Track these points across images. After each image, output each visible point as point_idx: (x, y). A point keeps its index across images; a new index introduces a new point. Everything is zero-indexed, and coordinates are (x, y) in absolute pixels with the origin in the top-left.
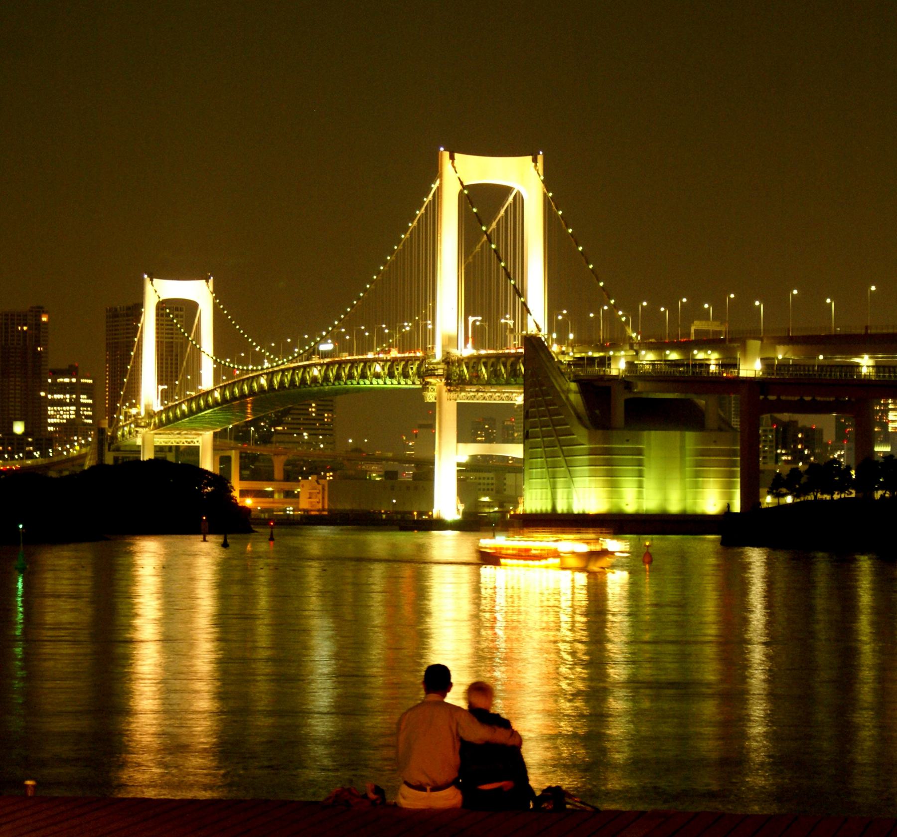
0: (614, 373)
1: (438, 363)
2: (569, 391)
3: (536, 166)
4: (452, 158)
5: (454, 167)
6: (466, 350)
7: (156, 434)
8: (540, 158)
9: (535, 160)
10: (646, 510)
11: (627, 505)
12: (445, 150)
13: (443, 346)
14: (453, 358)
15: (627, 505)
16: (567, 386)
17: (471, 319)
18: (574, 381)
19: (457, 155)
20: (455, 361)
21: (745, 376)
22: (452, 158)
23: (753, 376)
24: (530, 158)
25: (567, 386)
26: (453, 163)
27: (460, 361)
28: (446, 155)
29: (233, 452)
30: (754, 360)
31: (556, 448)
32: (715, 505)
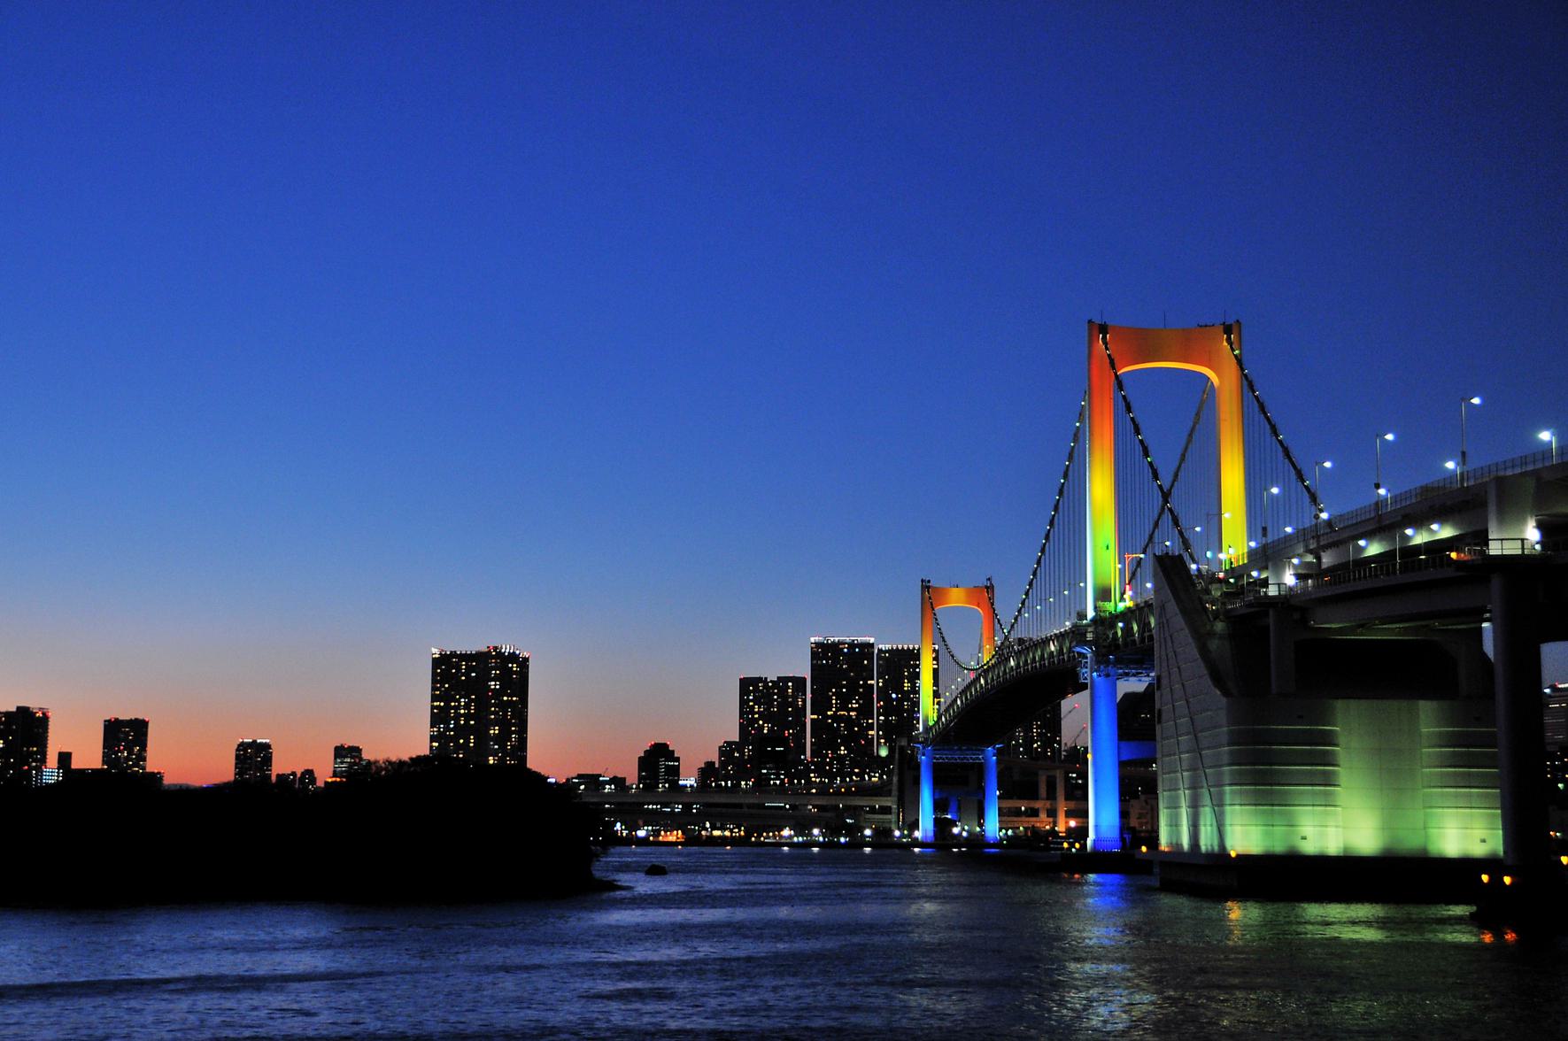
0: (1272, 591)
1: (1088, 625)
2: (1211, 634)
7: (935, 750)
10: (1345, 849)
11: (1304, 838)
14: (1102, 614)
15: (1304, 838)
16: (1208, 627)
17: (1129, 557)
20: (1105, 618)
21: (1499, 553)
23: (1520, 552)
25: (1208, 627)
29: (1058, 771)
30: (1523, 522)
32: (1483, 841)
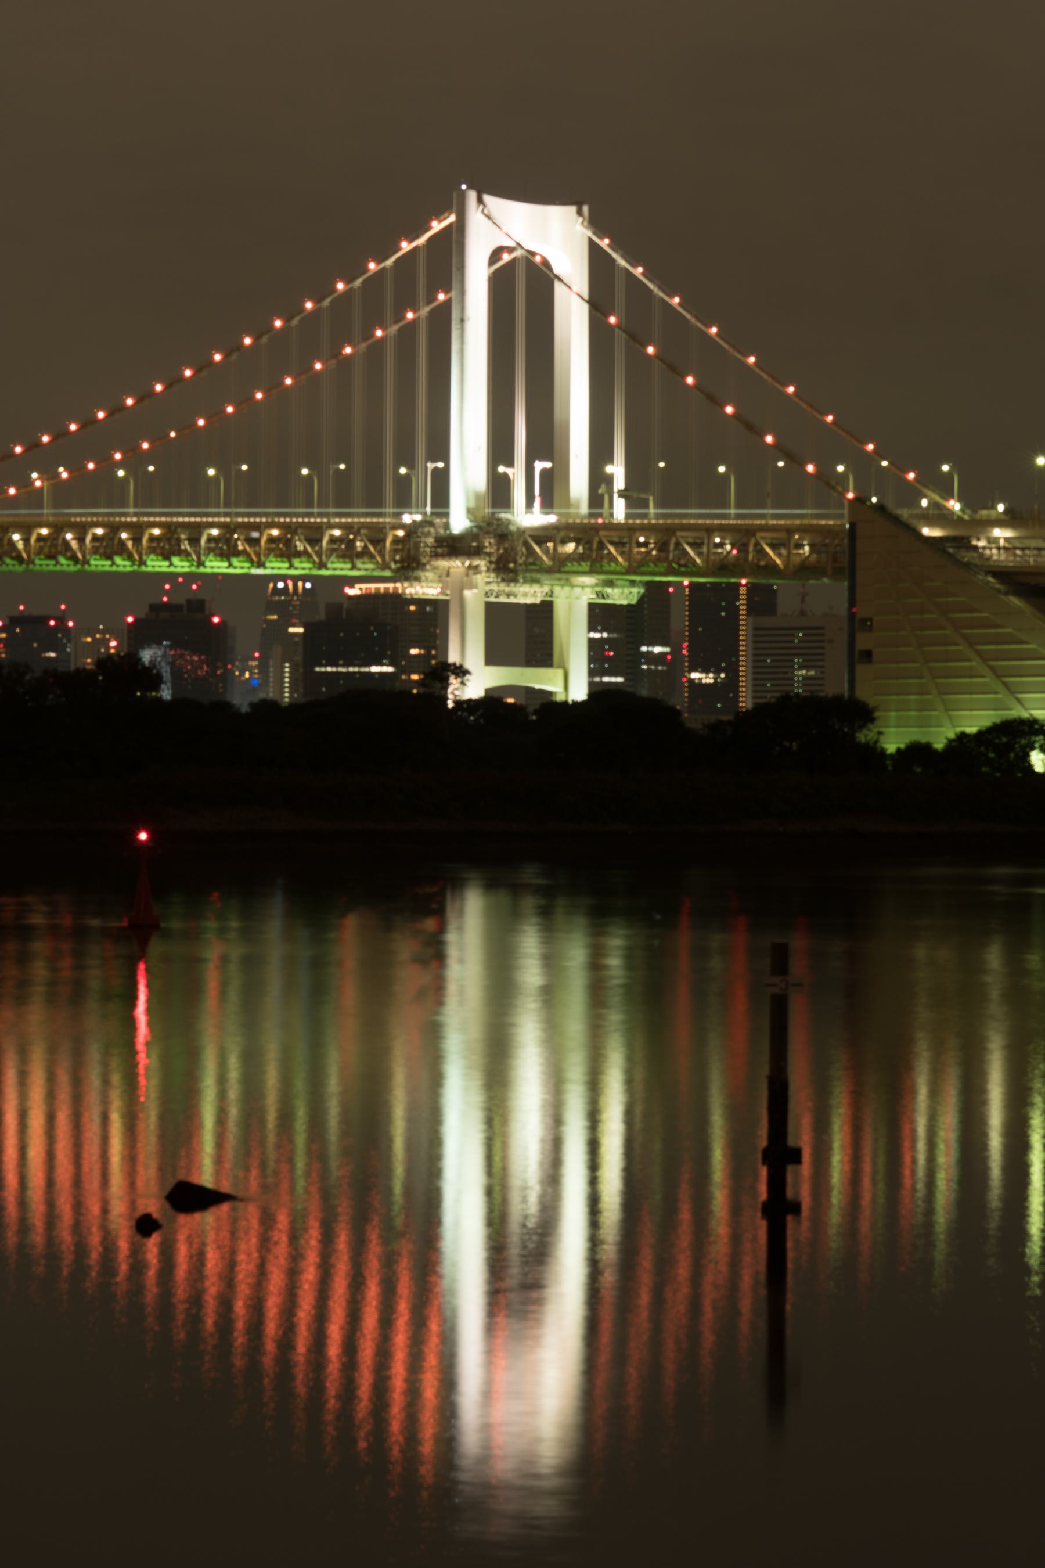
3: (583, 223)
4: (480, 201)
5: (489, 217)
6: (529, 515)
8: (585, 209)
9: (580, 213)
12: (469, 187)
13: (469, 511)
17: (539, 466)
18: (987, 573)
19: (487, 198)
22: (480, 201)
24: (572, 209)
26: (483, 211)
27: (522, 532)
28: (472, 196)
31: (924, 681)
